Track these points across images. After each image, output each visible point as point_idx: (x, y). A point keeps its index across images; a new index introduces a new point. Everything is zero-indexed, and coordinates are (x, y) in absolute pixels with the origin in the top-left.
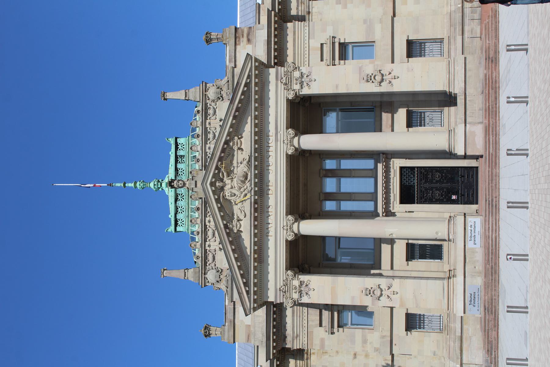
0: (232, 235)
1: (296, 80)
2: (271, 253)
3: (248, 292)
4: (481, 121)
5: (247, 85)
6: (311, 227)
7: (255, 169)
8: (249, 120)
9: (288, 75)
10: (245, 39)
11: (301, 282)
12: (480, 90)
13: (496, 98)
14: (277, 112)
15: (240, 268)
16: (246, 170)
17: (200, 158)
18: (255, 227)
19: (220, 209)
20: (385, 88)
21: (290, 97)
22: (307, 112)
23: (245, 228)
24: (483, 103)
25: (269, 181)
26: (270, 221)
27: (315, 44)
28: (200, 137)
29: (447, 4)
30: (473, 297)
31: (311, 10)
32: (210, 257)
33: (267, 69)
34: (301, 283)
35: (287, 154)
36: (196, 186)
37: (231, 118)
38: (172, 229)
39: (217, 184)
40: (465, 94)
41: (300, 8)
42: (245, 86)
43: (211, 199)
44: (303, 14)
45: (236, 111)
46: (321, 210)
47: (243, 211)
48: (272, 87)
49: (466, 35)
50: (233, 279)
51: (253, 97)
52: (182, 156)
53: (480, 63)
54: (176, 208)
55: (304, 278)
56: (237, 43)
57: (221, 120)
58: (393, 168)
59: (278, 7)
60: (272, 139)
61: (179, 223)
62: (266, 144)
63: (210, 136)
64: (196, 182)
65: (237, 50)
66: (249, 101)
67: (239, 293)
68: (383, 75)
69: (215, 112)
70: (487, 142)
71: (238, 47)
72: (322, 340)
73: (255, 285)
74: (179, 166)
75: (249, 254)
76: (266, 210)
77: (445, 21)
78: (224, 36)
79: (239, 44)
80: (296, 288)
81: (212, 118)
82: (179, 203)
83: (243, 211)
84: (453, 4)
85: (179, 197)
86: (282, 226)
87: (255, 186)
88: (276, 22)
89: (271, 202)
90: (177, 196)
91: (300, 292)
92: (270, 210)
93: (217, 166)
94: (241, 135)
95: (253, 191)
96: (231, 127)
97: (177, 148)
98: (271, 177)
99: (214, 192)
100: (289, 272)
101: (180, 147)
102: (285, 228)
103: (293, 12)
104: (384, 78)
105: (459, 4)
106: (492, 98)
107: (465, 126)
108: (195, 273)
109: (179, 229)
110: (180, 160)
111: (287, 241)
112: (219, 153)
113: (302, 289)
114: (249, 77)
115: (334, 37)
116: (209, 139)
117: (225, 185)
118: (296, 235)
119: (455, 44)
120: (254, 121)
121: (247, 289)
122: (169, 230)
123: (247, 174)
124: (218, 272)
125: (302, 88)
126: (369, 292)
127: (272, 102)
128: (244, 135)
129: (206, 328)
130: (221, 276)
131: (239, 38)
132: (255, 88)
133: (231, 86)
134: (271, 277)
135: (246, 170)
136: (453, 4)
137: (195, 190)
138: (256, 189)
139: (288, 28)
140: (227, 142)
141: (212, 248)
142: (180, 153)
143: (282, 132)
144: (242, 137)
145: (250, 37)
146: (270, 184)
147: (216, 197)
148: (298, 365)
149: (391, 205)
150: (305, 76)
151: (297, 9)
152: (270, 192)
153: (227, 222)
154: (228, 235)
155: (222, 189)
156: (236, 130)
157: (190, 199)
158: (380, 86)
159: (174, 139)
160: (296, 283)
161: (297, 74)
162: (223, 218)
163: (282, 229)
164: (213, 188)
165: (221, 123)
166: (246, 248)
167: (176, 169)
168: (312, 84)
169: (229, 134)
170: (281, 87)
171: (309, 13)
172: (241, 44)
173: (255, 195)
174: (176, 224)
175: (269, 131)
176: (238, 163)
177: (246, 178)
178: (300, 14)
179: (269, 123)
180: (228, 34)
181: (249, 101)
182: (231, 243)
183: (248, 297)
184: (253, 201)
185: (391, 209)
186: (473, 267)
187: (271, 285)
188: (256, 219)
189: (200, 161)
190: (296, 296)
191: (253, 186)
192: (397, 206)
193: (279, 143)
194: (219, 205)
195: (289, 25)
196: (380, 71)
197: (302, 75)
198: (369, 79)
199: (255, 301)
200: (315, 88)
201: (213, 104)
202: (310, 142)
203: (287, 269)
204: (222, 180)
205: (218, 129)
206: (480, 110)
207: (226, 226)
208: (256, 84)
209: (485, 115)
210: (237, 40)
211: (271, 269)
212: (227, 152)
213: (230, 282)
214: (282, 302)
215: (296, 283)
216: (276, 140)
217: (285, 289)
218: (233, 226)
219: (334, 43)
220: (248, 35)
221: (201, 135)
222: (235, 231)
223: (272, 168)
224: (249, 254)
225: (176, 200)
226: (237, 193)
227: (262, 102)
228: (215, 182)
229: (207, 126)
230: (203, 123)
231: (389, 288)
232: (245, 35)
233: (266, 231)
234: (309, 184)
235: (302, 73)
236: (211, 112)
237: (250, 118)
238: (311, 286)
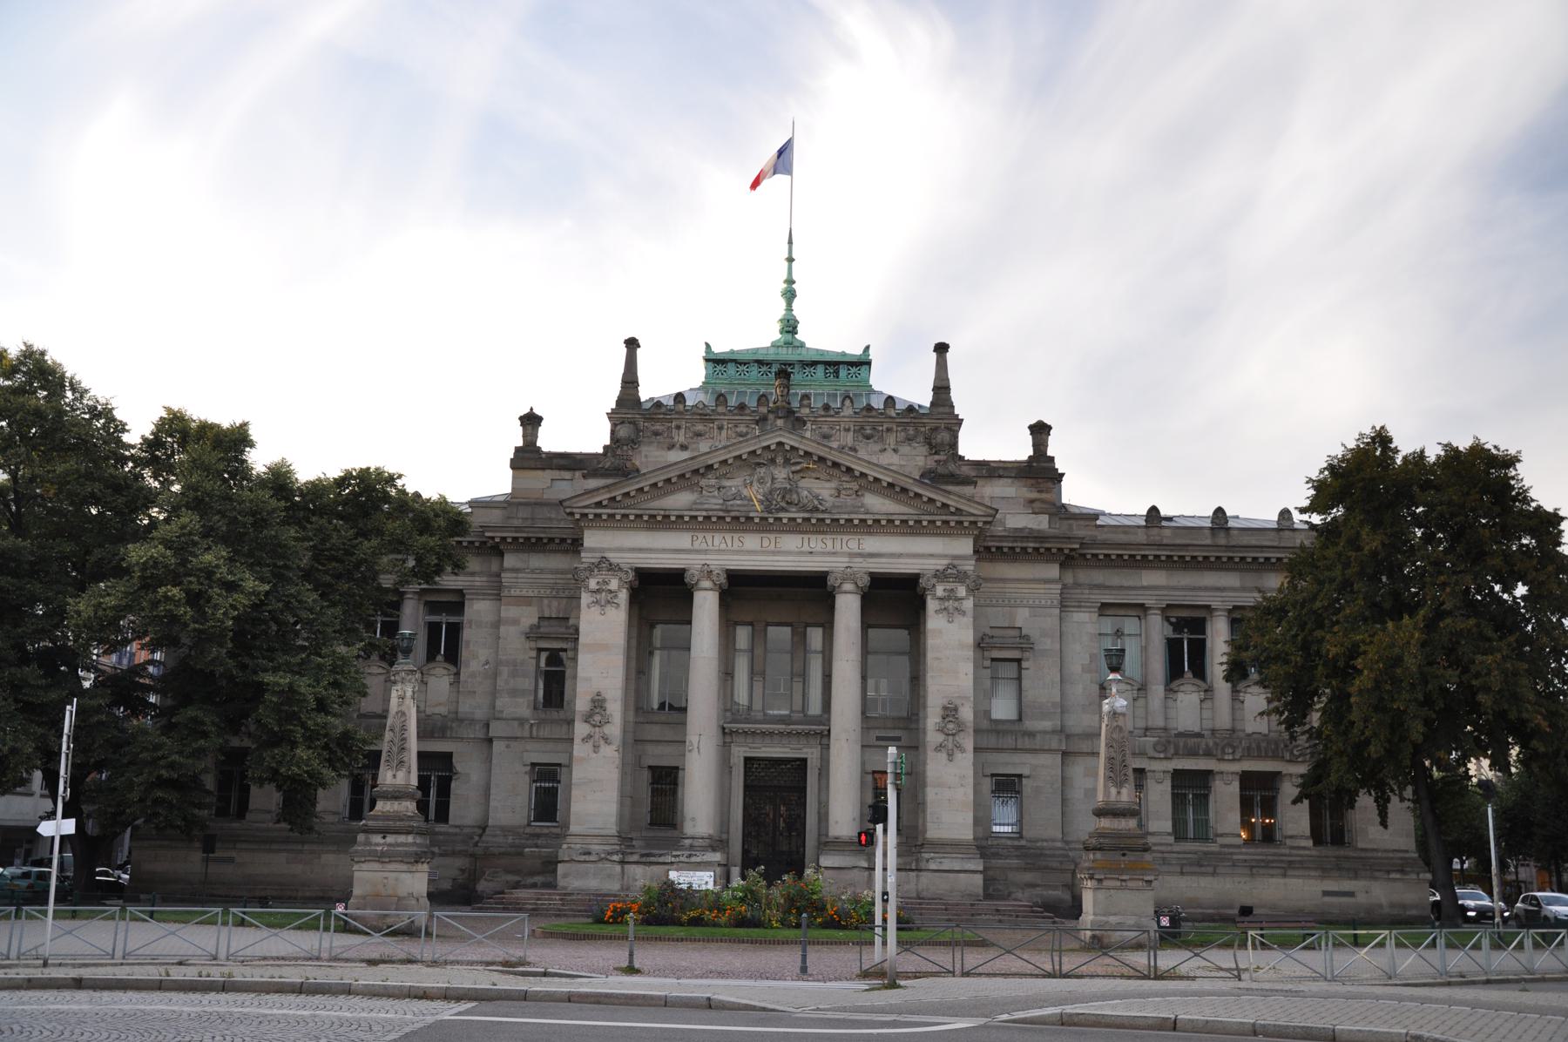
3: (599, 504)
5: (944, 505)
6: (706, 606)
9: (961, 577)
10: (1035, 495)
20: (933, 737)
27: (1022, 617)
32: (658, 427)
46: (737, 623)
55: (623, 596)
61: (719, 368)
67: (598, 489)
72: (516, 622)
74: (820, 368)
80: (606, 583)
82: (754, 369)
85: (764, 369)
91: (598, 591)
101: (853, 370)
111: (684, 570)
114: (959, 511)
126: (598, 703)
140: (849, 470)
142: (843, 372)
154: (696, 472)
160: (614, 584)
161: (962, 591)
167: (814, 364)
169: (863, 475)
170: (940, 564)
190: (593, 584)
192: (739, 752)
198: (950, 712)
199: (584, 515)
200: (935, 622)
202: (848, 609)
204: (787, 462)
207: (710, 467)
208: (946, 522)
217: (605, 565)
232: (1044, 496)
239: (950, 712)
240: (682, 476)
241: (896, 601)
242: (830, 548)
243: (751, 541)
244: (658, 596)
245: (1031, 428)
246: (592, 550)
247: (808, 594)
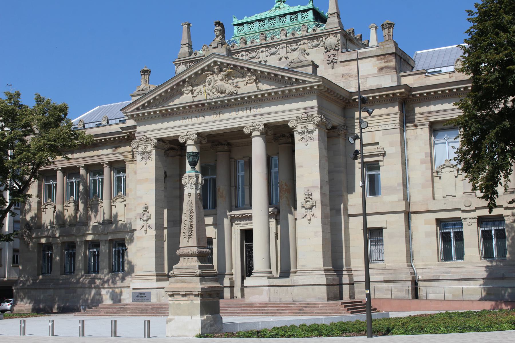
0: (180, 88)
1: (305, 127)
2: (171, 124)
3: (138, 109)
4: (271, 300)
5: (297, 80)
9: (308, 118)
10: (383, 65)
11: (151, 152)
12: (296, 299)
13: (267, 313)
14: (278, 112)
15: (154, 98)
16: (227, 92)
17: (275, 40)
18: (184, 107)
19: (196, 73)
21: (291, 125)
23: (186, 98)
24: (286, 301)
25: (223, 114)
26: (193, 119)
28: (292, 37)
29: (425, 265)
30: (143, 295)
31: (419, 127)
33: (316, 97)
34: (150, 153)
35: (243, 127)
36: (214, 48)
38: (236, 22)
39: (215, 68)
40: (294, 286)
41: (421, 116)
43: (203, 64)
44: (416, 120)
47: (203, 93)
48: (301, 105)
49: (384, 284)
50: (145, 94)
51: (286, 89)
52: (297, 17)
53: (319, 298)
54: (252, 22)
56: (379, 57)
57: (265, 62)
58: (248, 223)
59: (417, 94)
60: (255, 111)
61: (241, 27)
62: (252, 106)
63: (253, 54)
64: (217, 47)
65: (372, 59)
68: (311, 208)
69: (315, 47)
70: (250, 305)
71: (375, 59)
73: (143, 114)
74: (288, 17)
75: (169, 104)
76: (201, 114)
77: (401, 264)
78: (386, 42)
79: (378, 60)
80: (145, 148)
81: (247, 56)
82: (256, 24)
83: (203, 93)
84: (424, 270)
85: (262, 23)
86: (189, 130)
88: (394, 94)
89: (208, 118)
90: (263, 21)
91: (143, 153)
92: (202, 118)
94: (260, 82)
95: (210, 101)
98: (227, 115)
99: (209, 66)
100: (262, 127)
101: (305, 14)
102: (188, 133)
103: (417, 110)
104: (308, 210)
105: (422, 277)
106: (270, 310)
107: (268, 286)
108: (185, 54)
109: (236, 28)
112: (239, 64)
113: (145, 154)
115: (384, 155)
116: (291, 46)
117: (217, 74)
118: (460, 108)
119: (377, 274)
120: (266, 93)
121: (140, 108)
122: (234, 19)
123: (225, 93)
124: (336, 47)
125: (300, 133)
127: (288, 106)
128: (260, 85)
129: (146, 71)
130: (332, 50)
131: (384, 59)
132: (294, 89)
133: (296, 65)
134: (154, 126)
135: (227, 92)
136: (424, 270)
137: (211, 48)
138: (213, 104)
139: (394, 107)
140: (249, 69)
141: (260, 55)
142: (299, 15)
143: (262, 119)
144: (55, 117)
145: (385, 70)
146: (221, 115)
147: (206, 68)
148: (128, 154)
149: (239, 222)
150: (309, 135)
151: (420, 113)
152: (215, 116)
153: (188, 82)
154: (178, 85)
155: (214, 73)
156: (260, 77)
157: (280, 29)
158: (302, 207)
159: (311, 7)
160: (149, 148)
161: (310, 127)
162: (190, 77)
163: (187, 131)
164: (212, 64)
165: (263, 62)
166: (173, 102)
167: (285, 15)
168: (303, 143)
169: (255, 71)
170: (300, 113)
171: (416, 126)
172: (378, 62)
175: (263, 108)
176: (237, 82)
177: (221, 93)
178: (416, 117)
179: (270, 107)
180: (388, 46)
181: (286, 85)
182: (172, 88)
183: (134, 109)
184: (203, 102)
185: (236, 222)
186: (163, 295)
187: (148, 127)
188: (190, 107)
189: (272, 41)
190: (140, 149)
191: (214, 100)
193: (253, 118)
194: (200, 72)
195: (396, 109)
196: (315, 206)
197: (309, 132)
198: (309, 196)
201: (322, 44)
203: (265, 125)
204: (221, 71)
205: (257, 61)
206: (280, 299)
207: (184, 81)
208: (297, 89)
209: (263, 304)
210: (382, 57)
211: (160, 125)
212: (242, 72)
214: (137, 138)
215: (149, 148)
216: (255, 116)
218: (186, 87)
219: (377, 155)
220: (387, 67)
221: (295, 37)
222: (183, 90)
223: (234, 115)
224: (169, 104)
225: (259, 20)
226: (211, 86)
228: (218, 65)
229: (303, 42)
230: (304, 37)
231: (149, 227)
232: (387, 64)
233: (186, 117)
234: (224, 150)
235: (312, 131)
236: (316, 42)
237: (274, 87)
238: (148, 161)
239: (309, 196)
241: (281, 138)
244: (171, 151)
246: (139, 133)
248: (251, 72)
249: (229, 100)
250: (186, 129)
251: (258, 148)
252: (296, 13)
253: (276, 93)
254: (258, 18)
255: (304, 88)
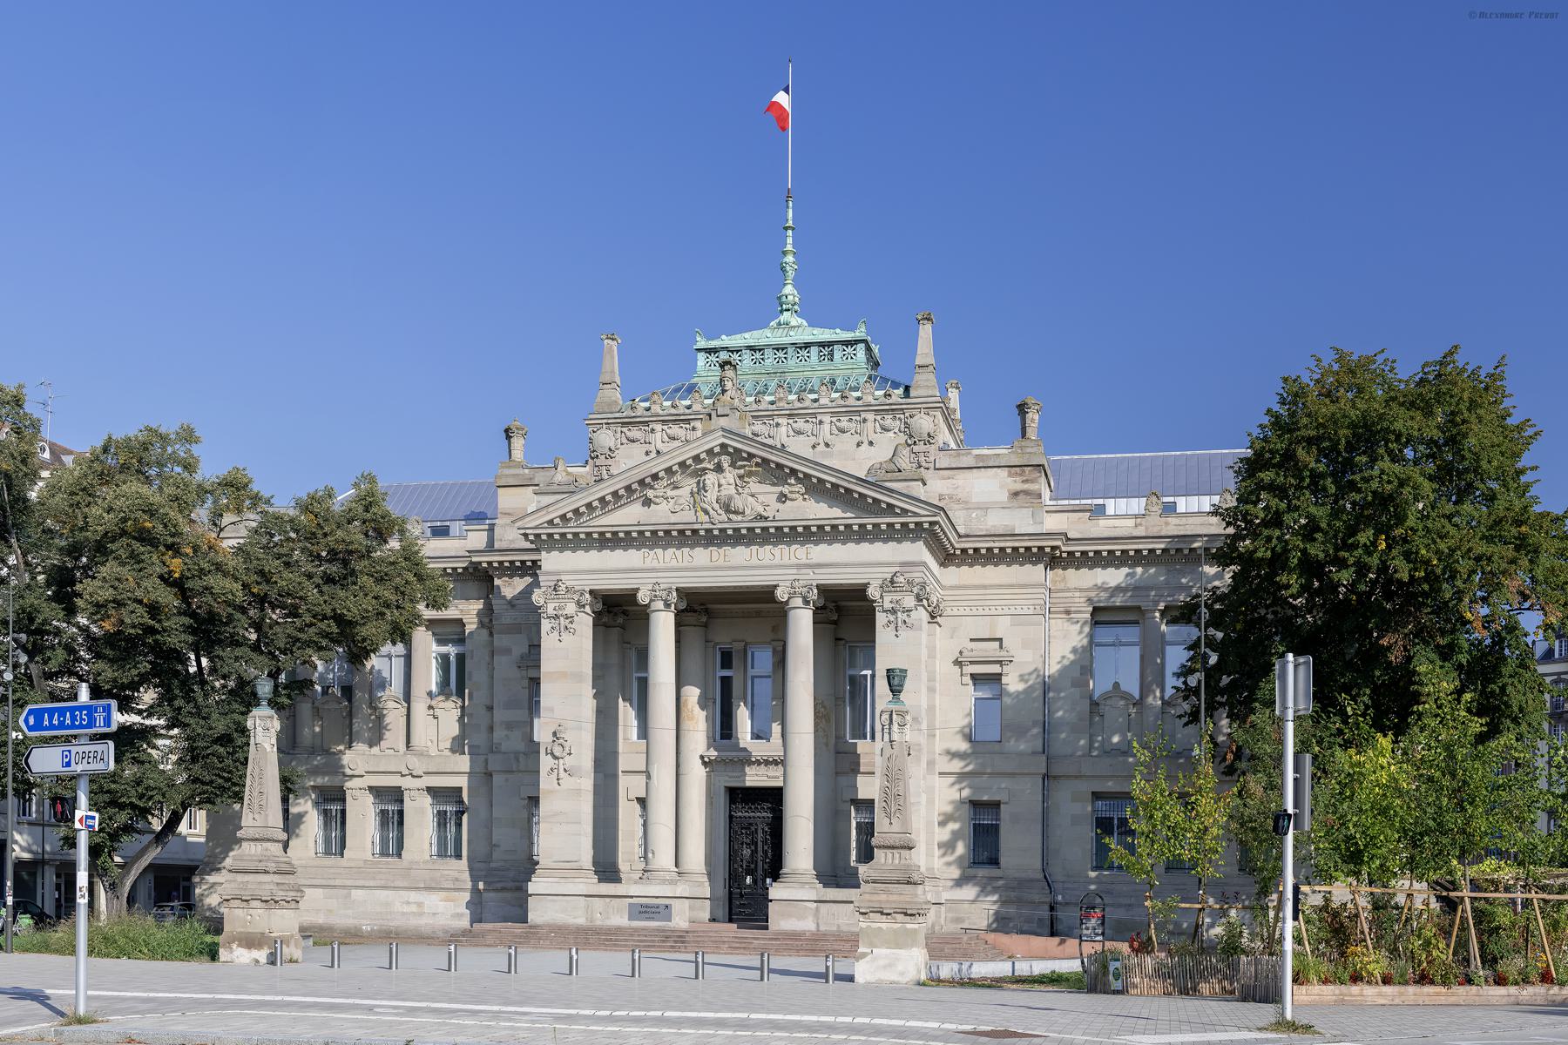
7: (749, 529)
8: (836, 512)
16: (748, 512)
18: (654, 533)
22: (846, 616)
32: (635, 433)
35: (776, 586)
37: (833, 480)
42: (889, 505)
45: (847, 490)
51: (869, 521)
52: (831, 354)
66: (869, 509)
74: (814, 350)
82: (747, 355)
85: (758, 355)
87: (721, 530)
93: (754, 456)
96: (819, 480)
97: (847, 343)
101: (850, 350)
109: (701, 357)
110: (825, 351)
114: (905, 512)
142: (837, 355)
156: (817, 489)
167: (807, 346)
173: (707, 531)
174: (709, 351)
181: (869, 509)
213: (566, 488)
225: (752, 348)
227: (864, 535)
240: (628, 488)
242: (777, 561)
243: (701, 555)
245: (1019, 406)
247: (760, 608)
248: (797, 479)
249: (750, 530)
250: (654, 575)
251: (802, 626)
252: (830, 344)
253: (848, 526)
254: (752, 343)
255: (904, 525)
